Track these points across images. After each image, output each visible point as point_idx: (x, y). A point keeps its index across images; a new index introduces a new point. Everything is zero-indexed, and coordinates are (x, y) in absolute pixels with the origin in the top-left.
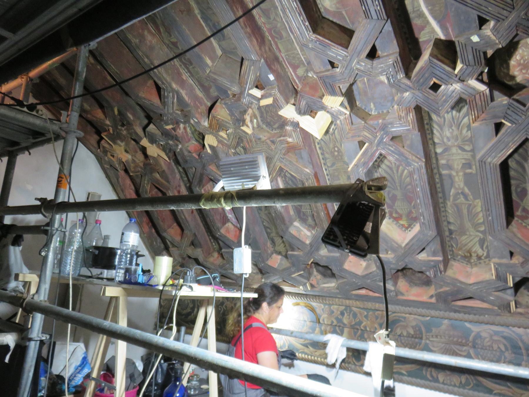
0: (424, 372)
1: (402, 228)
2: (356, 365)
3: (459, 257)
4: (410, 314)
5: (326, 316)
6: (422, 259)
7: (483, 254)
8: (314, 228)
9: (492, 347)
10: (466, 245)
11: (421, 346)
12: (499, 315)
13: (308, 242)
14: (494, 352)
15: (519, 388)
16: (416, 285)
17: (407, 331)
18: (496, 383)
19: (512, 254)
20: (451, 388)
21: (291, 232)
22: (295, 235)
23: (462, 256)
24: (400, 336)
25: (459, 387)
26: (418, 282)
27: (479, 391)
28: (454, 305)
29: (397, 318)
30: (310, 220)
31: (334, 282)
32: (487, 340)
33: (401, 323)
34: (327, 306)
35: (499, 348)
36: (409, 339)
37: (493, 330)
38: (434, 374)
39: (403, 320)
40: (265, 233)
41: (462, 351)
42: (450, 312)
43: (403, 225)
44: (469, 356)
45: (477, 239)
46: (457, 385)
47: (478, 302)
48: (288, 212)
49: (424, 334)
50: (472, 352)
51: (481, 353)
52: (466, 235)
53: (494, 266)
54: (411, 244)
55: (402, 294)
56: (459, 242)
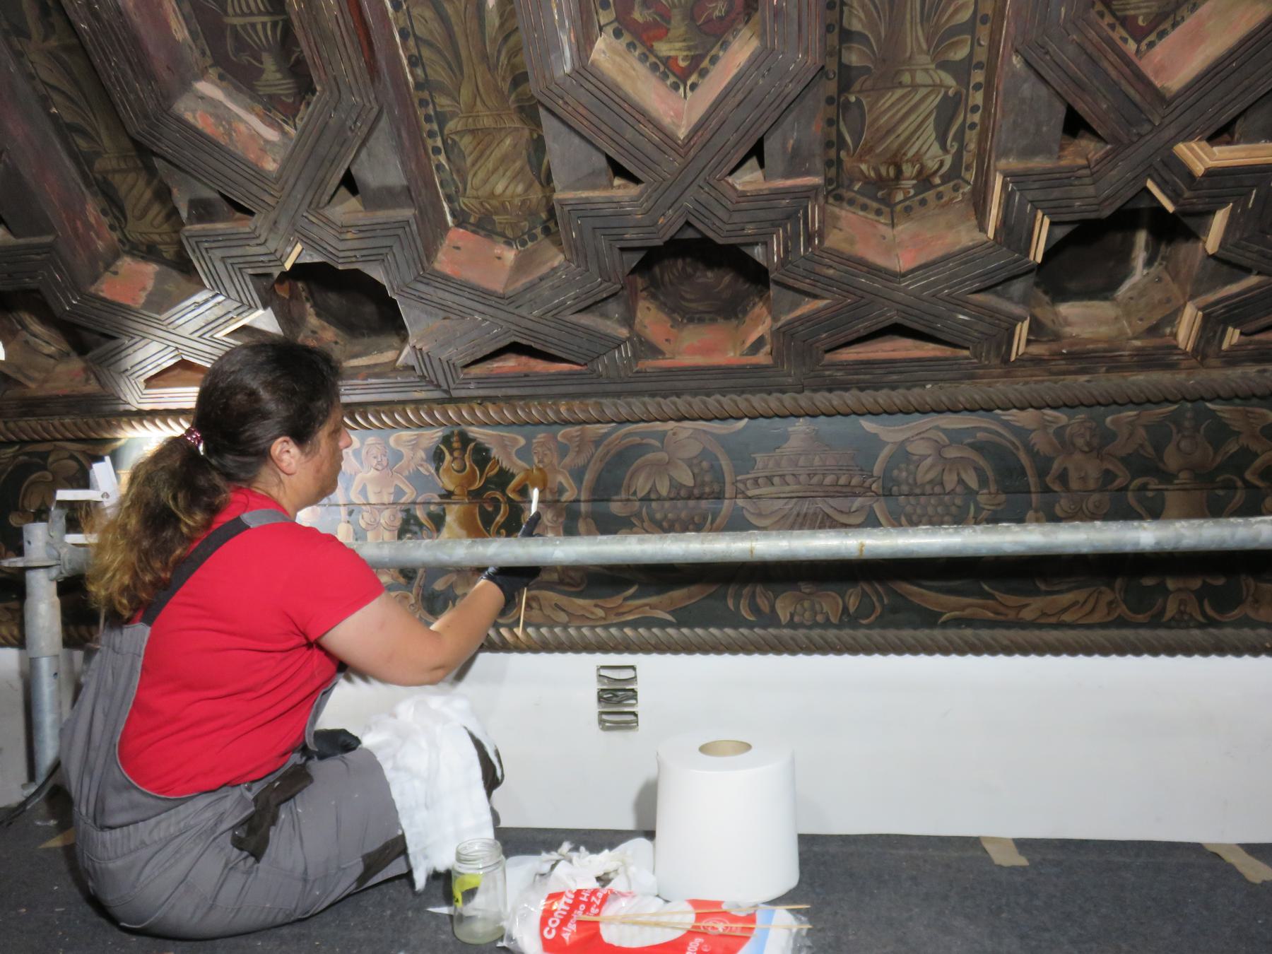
0: (730, 603)
1: (664, 76)
3: (856, 187)
5: (373, 473)
6: (748, 188)
7: (942, 164)
8: (291, 113)
9: (942, 484)
10: (889, 132)
11: (718, 520)
12: (972, 377)
13: (271, 166)
14: (947, 498)
15: (1009, 591)
16: (691, 320)
17: (671, 479)
18: (950, 592)
19: (1075, 125)
20: (815, 633)
21: (189, 117)
22: (208, 130)
23: (867, 180)
24: (646, 499)
25: (839, 626)
27: (898, 626)
28: (833, 365)
29: (637, 439)
30: (272, 73)
31: (390, 347)
32: (929, 461)
33: (650, 456)
34: (371, 440)
35: (961, 481)
36: (680, 504)
37: (945, 431)
38: (763, 603)
39: (657, 444)
40: (68, 162)
41: (849, 513)
42: (815, 391)
43: (667, 61)
44: (872, 522)
45: (933, 101)
46: (834, 620)
47: (909, 342)
49: (728, 479)
50: (879, 508)
51: (909, 509)
52: (901, 85)
53: (1005, 185)
54: (714, 123)
55: (655, 351)
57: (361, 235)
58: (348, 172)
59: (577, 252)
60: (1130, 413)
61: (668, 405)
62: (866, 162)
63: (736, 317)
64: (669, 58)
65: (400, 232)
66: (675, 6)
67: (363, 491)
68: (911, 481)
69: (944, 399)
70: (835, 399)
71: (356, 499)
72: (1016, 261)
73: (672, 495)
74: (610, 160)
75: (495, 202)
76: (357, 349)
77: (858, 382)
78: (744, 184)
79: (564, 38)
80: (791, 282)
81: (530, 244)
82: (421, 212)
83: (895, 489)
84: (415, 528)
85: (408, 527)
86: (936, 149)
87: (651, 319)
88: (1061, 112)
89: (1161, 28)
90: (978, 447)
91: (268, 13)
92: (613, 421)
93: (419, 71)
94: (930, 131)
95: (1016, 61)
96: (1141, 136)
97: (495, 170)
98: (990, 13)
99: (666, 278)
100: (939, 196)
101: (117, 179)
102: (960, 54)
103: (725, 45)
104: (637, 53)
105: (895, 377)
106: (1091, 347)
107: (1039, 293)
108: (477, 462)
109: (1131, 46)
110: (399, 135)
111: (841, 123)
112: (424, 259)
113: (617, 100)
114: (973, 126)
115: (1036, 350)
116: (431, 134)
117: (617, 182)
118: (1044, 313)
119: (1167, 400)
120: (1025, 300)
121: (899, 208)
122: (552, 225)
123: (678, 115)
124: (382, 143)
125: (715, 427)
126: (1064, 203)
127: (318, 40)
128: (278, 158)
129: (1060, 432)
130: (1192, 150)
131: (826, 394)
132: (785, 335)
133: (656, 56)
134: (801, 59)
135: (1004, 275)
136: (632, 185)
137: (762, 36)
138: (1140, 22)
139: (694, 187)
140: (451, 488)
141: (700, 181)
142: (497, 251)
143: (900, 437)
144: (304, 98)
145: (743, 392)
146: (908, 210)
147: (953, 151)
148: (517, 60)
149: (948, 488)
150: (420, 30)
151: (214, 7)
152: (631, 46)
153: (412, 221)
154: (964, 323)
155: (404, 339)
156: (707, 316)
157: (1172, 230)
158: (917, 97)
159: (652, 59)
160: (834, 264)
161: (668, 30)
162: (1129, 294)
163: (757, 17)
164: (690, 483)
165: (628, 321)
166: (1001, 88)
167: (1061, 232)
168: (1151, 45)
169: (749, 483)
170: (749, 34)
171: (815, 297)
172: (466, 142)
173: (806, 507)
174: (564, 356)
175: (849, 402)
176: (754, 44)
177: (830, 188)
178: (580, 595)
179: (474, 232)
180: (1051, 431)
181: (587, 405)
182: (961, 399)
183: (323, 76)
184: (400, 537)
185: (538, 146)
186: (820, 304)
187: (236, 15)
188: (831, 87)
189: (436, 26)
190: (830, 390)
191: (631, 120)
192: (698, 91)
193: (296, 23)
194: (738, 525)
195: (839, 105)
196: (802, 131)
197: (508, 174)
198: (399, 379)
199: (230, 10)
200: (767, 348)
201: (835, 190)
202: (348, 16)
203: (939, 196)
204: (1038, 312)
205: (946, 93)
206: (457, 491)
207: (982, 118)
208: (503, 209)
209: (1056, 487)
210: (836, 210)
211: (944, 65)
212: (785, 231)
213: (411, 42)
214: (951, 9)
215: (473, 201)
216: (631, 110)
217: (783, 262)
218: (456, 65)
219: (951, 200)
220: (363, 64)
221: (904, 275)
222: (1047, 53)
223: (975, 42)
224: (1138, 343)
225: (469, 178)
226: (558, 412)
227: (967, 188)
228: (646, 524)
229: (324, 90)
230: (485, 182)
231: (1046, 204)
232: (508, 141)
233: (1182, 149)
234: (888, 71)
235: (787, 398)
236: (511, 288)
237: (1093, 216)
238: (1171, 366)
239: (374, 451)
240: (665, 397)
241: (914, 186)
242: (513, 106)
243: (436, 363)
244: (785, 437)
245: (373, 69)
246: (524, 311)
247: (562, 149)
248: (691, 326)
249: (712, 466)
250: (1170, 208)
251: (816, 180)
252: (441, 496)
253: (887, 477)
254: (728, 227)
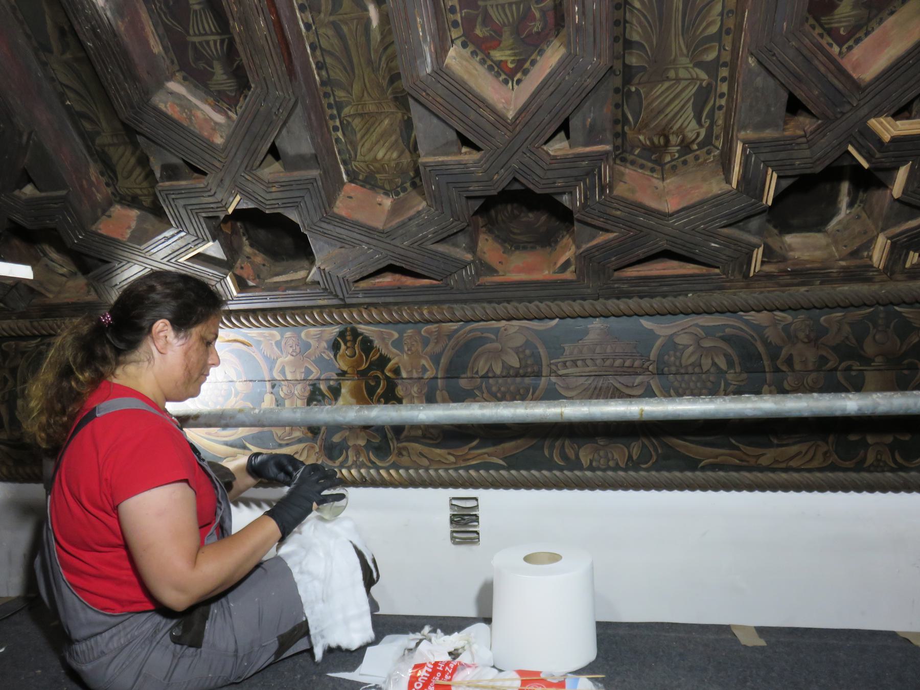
0: (546, 453)
2: (378, 469)
3: (637, 152)
4: (510, 319)
5: (289, 358)
7: (698, 135)
8: (233, 103)
10: (660, 112)
12: (721, 288)
13: (219, 140)
14: (704, 376)
15: (749, 445)
16: (517, 248)
17: (503, 362)
19: (794, 106)
21: (162, 106)
23: (644, 148)
24: (486, 377)
25: (626, 470)
26: (523, 238)
27: (669, 469)
28: (620, 280)
29: (479, 334)
30: (219, 74)
31: (302, 268)
32: (691, 349)
33: (488, 346)
34: (288, 334)
35: (714, 364)
36: (509, 380)
37: (702, 327)
38: (571, 453)
39: (493, 337)
40: (77, 139)
43: (500, 64)
44: (649, 394)
45: (692, 90)
46: (622, 465)
47: (675, 263)
48: (144, 42)
49: (544, 363)
50: (654, 384)
52: (668, 79)
53: (744, 150)
54: (533, 108)
55: (492, 271)
56: (645, 103)
57: (282, 189)
58: (273, 144)
59: (436, 199)
60: (839, 315)
61: (501, 309)
62: (644, 134)
63: (550, 245)
64: (501, 61)
65: (310, 186)
66: (504, 25)
67: (283, 372)
68: (678, 364)
69: (701, 304)
70: (622, 304)
71: (277, 376)
72: (753, 204)
73: (504, 374)
74: (459, 135)
75: (377, 165)
76: (278, 269)
77: (639, 292)
78: (556, 150)
79: (426, 49)
80: (589, 220)
81: (402, 194)
82: (324, 172)
83: (666, 369)
84: (320, 398)
85: (314, 396)
86: (694, 124)
87: (488, 247)
88: (784, 97)
89: (857, 36)
90: (726, 339)
91: (218, 34)
92: (461, 321)
93: (324, 73)
94: (689, 112)
95: (751, 60)
96: (843, 114)
97: (378, 141)
98: (732, 27)
99: (500, 218)
100: (697, 158)
101: (111, 151)
102: (711, 56)
103: (541, 52)
104: (478, 59)
105: (665, 288)
106: (808, 266)
107: (770, 227)
108: (363, 350)
109: (836, 49)
110: (310, 118)
111: (625, 107)
112: (327, 206)
113: (464, 91)
114: (720, 108)
115: (768, 268)
116: (332, 117)
117: (464, 150)
118: (774, 242)
119: (865, 305)
120: (760, 233)
121: (667, 166)
122: (417, 180)
123: (508, 102)
124: (297, 124)
125: (535, 325)
126: (788, 162)
127: (253, 52)
128: (224, 134)
129: (786, 328)
130: (881, 123)
131: (615, 301)
132: (585, 258)
133: (492, 61)
134: (595, 62)
135: (744, 214)
136: (474, 152)
137: (568, 45)
138: (842, 32)
139: (520, 153)
140: (345, 368)
141: (523, 149)
142: (379, 199)
143: (670, 332)
144: (242, 93)
145: (555, 300)
146: (674, 168)
147: (707, 124)
148: (393, 64)
150: (324, 43)
151: (180, 29)
152: (474, 53)
153: (318, 178)
154: (715, 249)
155: (312, 262)
156: (529, 245)
157: (868, 181)
158: (680, 88)
159: (489, 62)
160: (621, 208)
161: (500, 42)
162: (837, 228)
163: (564, 32)
164: (517, 365)
165: (472, 248)
166: (740, 80)
167: (786, 183)
168: (850, 48)
169: (559, 365)
170: (558, 44)
171: (607, 231)
172: (357, 123)
173: (600, 382)
174: (426, 274)
175: (632, 307)
176: (562, 51)
177: (618, 153)
178: (437, 446)
179: (362, 186)
180: (780, 327)
181: (442, 309)
182: (714, 304)
183: (256, 76)
184: (308, 404)
185: (408, 125)
186: (611, 236)
187: (195, 35)
188: (618, 81)
189: (335, 41)
190: (618, 298)
191: (475, 106)
192: (521, 85)
193: (237, 39)
194: (552, 395)
195: (624, 94)
196: (598, 112)
197: (387, 144)
198: (309, 291)
199: (191, 32)
200: (572, 268)
201: (621, 154)
202: (274, 35)
203: (697, 158)
204: (770, 241)
205: (701, 84)
206: (349, 371)
207: (727, 101)
208: (382, 169)
209: (784, 368)
210: (622, 169)
211: (699, 65)
212: (585, 184)
213: (318, 53)
214: (704, 24)
215: (362, 164)
216: (473, 99)
217: (584, 206)
218: (349, 68)
219: (705, 160)
220: (284, 68)
221: (671, 215)
222: (774, 55)
223: (722, 48)
224: (843, 263)
225: (359, 148)
226: (422, 314)
227: (717, 152)
228: (485, 395)
229: (256, 87)
230: (370, 150)
231: (774, 163)
232: (386, 122)
233: (873, 123)
234: (659, 69)
235: (587, 304)
236: (389, 225)
237: (808, 171)
238: (869, 280)
239: (291, 342)
240: (499, 303)
241: (678, 151)
242: (390, 97)
243: (335, 280)
244: (586, 332)
245: (291, 72)
246: (397, 242)
247: (425, 127)
248: (517, 252)
249: (533, 354)
250: (866, 165)
251: (608, 147)
252: (338, 375)
253: (660, 361)
254: (544, 182)
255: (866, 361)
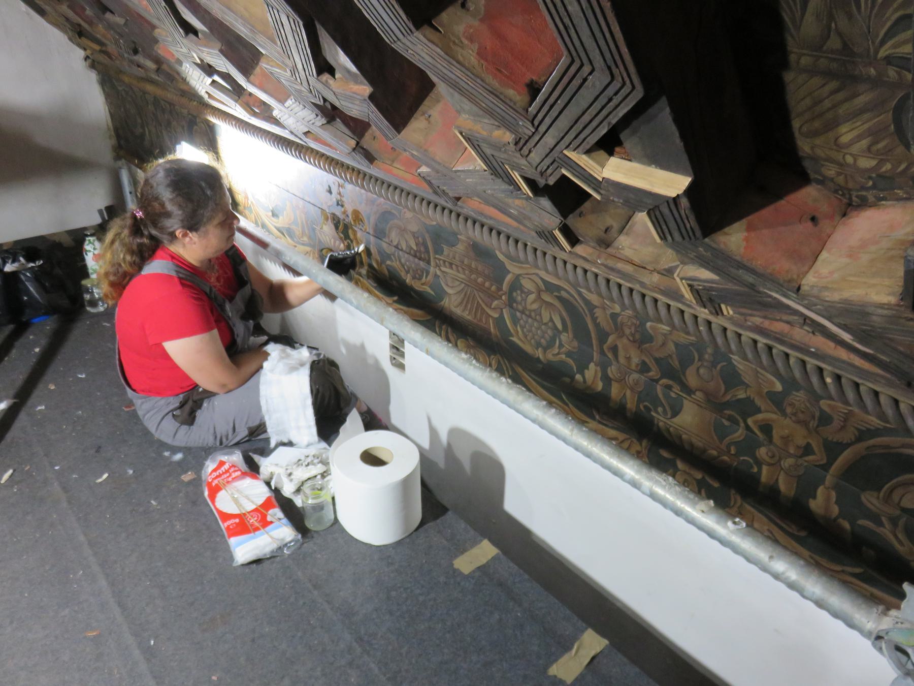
9: (540, 315)
14: (543, 327)
35: (551, 320)
149: (545, 321)
255: (689, 391)
